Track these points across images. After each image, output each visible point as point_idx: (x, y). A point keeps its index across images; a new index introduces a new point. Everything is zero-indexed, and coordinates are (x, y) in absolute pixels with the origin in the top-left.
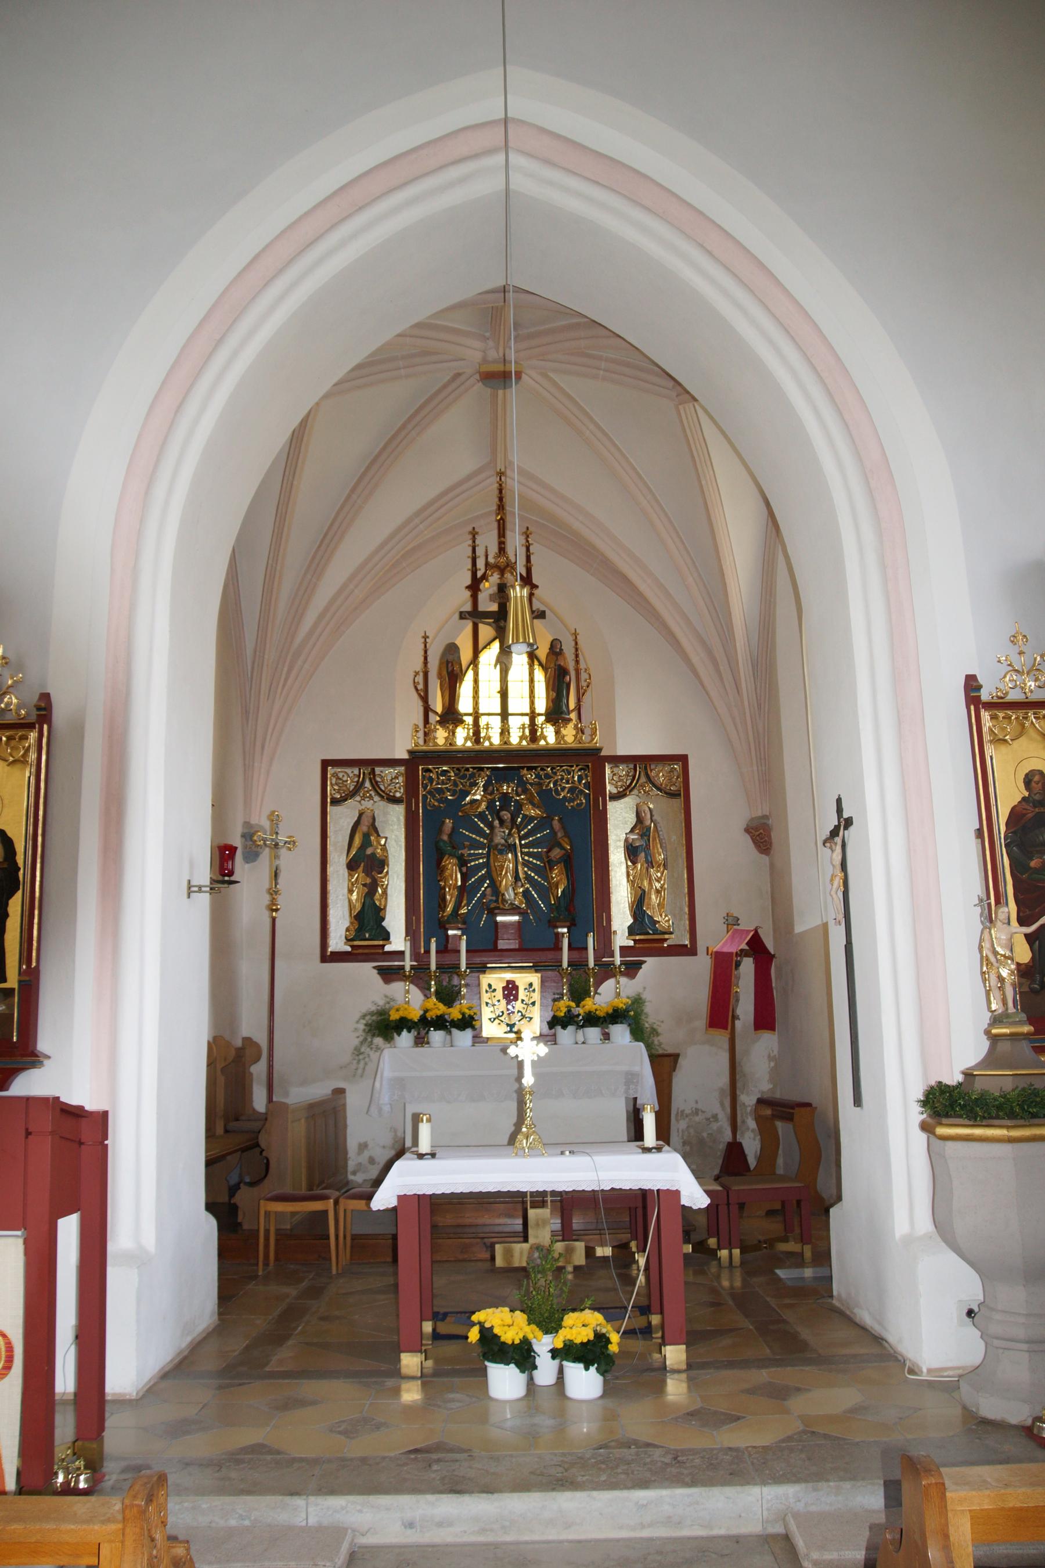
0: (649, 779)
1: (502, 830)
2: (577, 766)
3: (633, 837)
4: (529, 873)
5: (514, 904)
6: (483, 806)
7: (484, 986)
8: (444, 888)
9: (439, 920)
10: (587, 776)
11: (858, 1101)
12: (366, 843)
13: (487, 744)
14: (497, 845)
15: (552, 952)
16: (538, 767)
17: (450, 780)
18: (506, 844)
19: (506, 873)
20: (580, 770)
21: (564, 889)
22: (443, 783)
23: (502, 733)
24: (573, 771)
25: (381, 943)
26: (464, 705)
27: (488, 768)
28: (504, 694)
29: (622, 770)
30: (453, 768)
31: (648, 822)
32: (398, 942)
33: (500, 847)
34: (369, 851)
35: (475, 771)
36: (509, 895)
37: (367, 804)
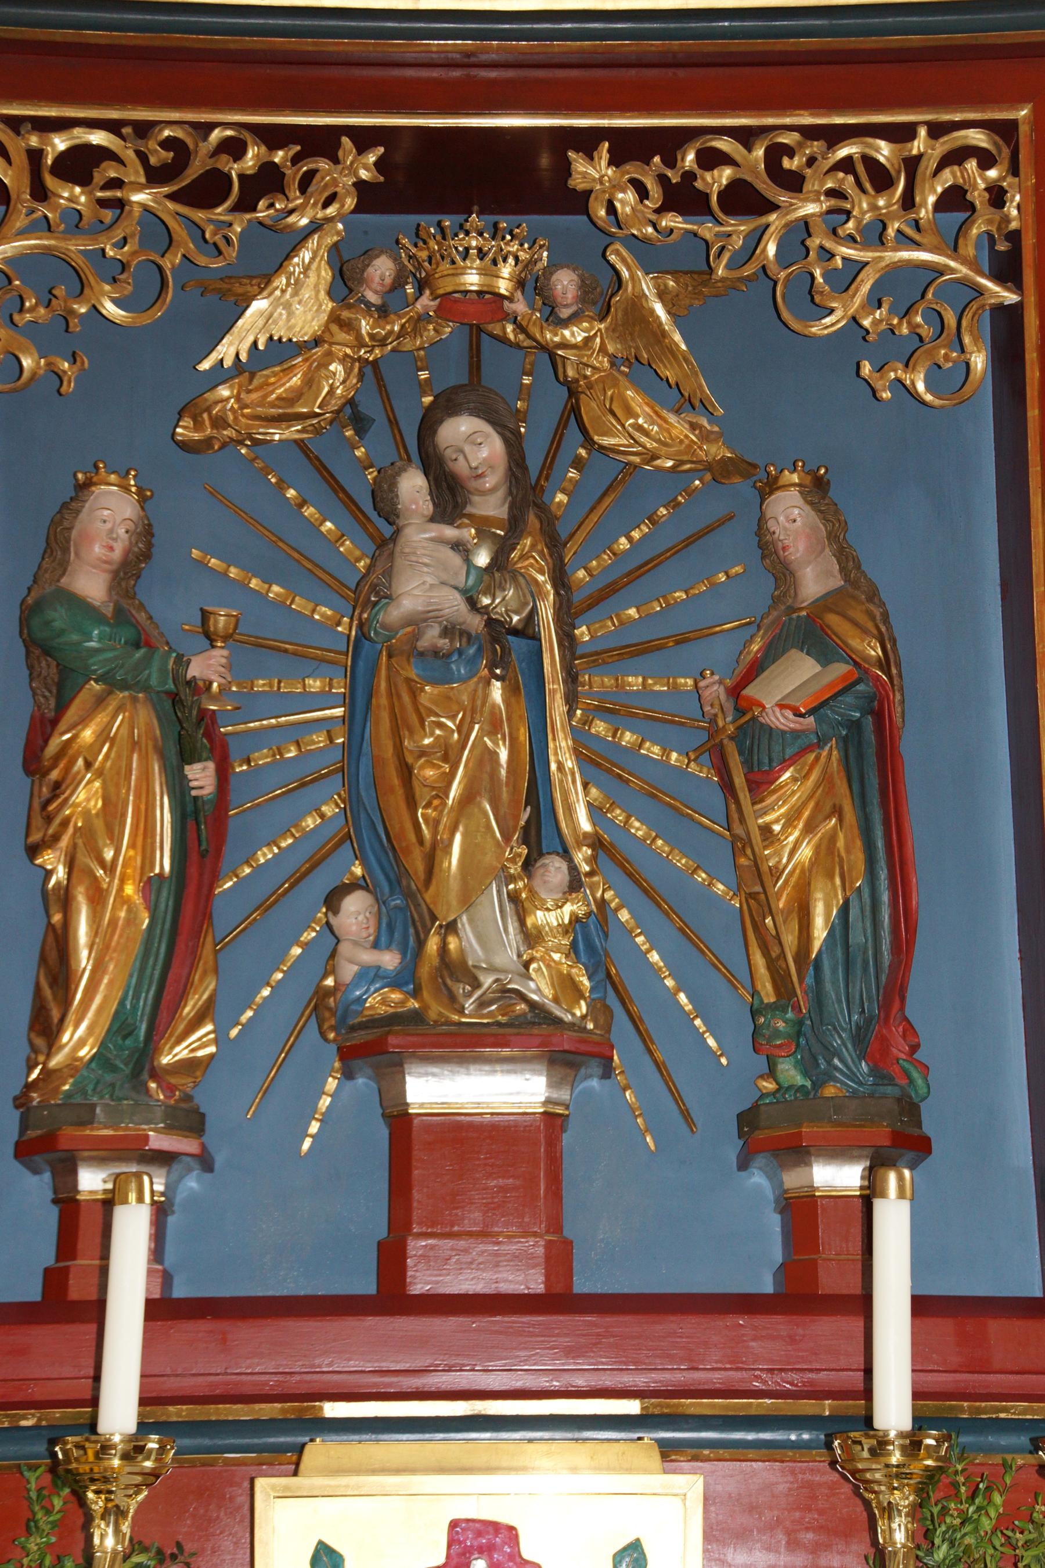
1: (450, 532)
2: (937, 131)
4: (618, 815)
5: (522, 997)
8: (65, 899)
9: (21, 1101)
10: (997, 196)
14: (417, 622)
15: (779, 1324)
16: (689, 134)
17: (120, 204)
18: (476, 623)
19: (468, 798)
20: (956, 157)
21: (845, 909)
22: (75, 222)
24: (912, 164)
27: (365, 139)
30: (143, 129)
33: (431, 636)
35: (278, 157)
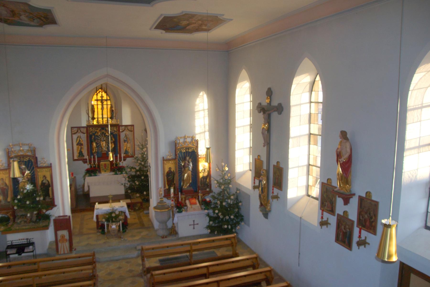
0: (128, 129)
3: (125, 138)
6: (99, 134)
7: (101, 165)
11: (151, 198)
12: (80, 141)
13: (100, 124)
23: (102, 122)
25: (82, 157)
26: (96, 116)
28: (102, 115)
29: (123, 127)
31: (127, 136)
32: (86, 157)
34: (80, 142)
36: (104, 149)
37: (79, 134)
